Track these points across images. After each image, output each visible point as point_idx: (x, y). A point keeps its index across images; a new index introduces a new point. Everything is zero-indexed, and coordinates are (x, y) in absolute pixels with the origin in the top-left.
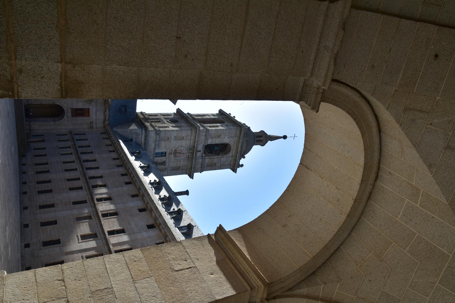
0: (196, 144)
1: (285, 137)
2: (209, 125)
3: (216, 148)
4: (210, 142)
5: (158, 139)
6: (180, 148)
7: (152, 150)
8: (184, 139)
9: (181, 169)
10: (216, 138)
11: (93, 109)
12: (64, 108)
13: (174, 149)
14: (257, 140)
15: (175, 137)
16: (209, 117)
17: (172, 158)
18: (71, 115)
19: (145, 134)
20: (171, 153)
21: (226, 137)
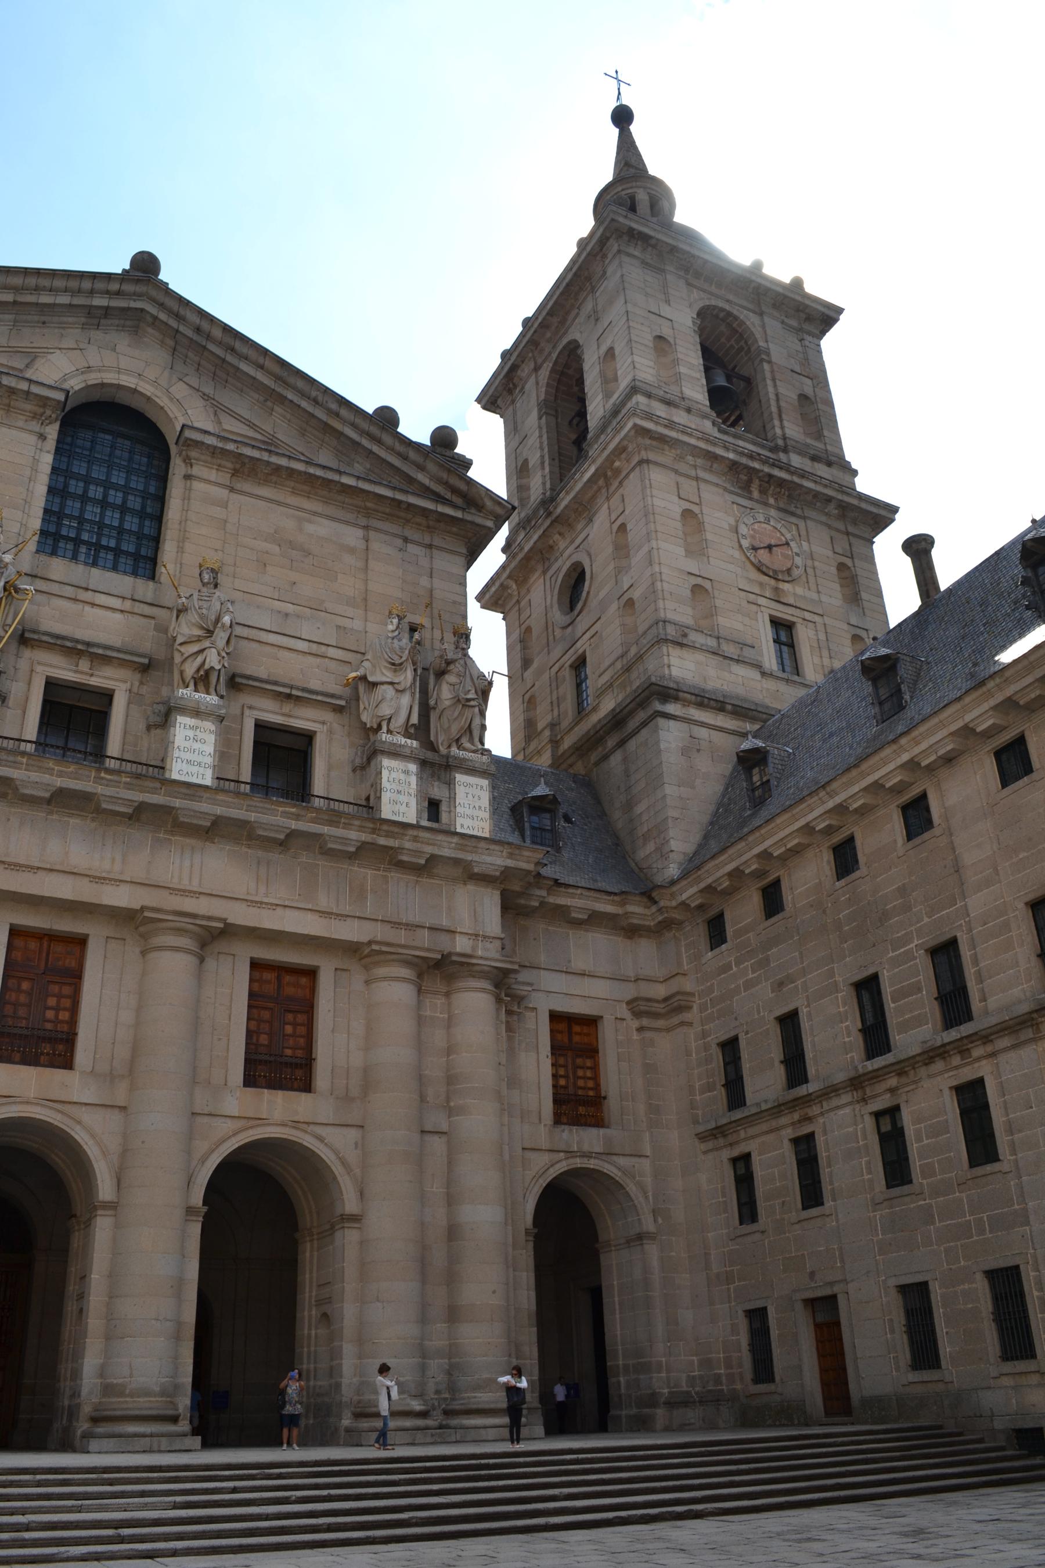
0: (720, 452)
1: (622, 117)
3: (721, 381)
4: (697, 393)
5: (712, 643)
6: (745, 543)
7: (770, 684)
8: (696, 509)
10: (676, 362)
11: (554, 992)
12: (553, 1173)
13: (754, 575)
15: (689, 553)
16: (533, 440)
17: (799, 591)
18: (593, 1132)
19: (687, 703)
20: (776, 589)
21: (666, 311)
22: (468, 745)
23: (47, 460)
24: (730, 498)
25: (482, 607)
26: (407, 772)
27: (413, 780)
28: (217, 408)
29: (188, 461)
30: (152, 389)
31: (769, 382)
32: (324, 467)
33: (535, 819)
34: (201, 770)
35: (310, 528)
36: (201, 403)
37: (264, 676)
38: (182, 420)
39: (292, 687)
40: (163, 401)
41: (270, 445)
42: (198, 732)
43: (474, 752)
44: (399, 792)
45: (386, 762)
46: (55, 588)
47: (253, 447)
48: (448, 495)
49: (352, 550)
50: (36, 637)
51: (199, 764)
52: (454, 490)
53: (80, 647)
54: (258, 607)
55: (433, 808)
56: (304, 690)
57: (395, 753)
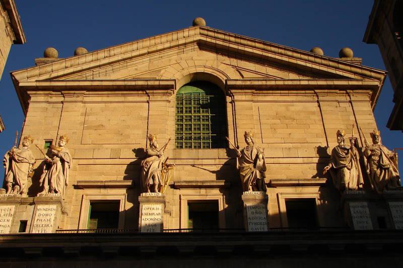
23: (172, 111)
25: (391, 129)
26: (363, 207)
27: (367, 210)
29: (231, 95)
30: (211, 70)
32: (292, 80)
34: (262, 226)
35: (292, 108)
37: (285, 178)
38: (225, 78)
39: (299, 180)
41: (267, 77)
42: (257, 209)
43: (395, 190)
44: (361, 217)
45: (351, 204)
46: (185, 162)
47: (258, 80)
48: (352, 76)
49: (313, 113)
50: (179, 184)
51: (261, 224)
52: (355, 73)
53: (199, 184)
54: (276, 148)
56: (305, 180)
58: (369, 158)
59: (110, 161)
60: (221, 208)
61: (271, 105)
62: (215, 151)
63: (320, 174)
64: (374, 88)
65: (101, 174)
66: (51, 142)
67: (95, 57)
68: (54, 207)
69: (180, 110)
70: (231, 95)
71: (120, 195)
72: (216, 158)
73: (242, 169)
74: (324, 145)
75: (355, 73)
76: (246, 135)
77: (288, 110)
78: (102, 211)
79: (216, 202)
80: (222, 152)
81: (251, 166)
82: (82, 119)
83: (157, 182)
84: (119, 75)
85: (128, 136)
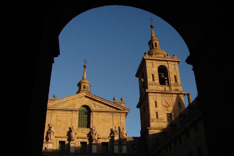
2: (145, 83)
9: (179, 101)
14: (156, 47)
21: (153, 69)
22: (124, 142)
23: (78, 116)
24: (161, 97)
27: (118, 148)
28: (95, 105)
29: (92, 113)
31: (169, 75)
33: (135, 146)
35: (106, 117)
36: (93, 104)
40: (89, 105)
45: (115, 146)
48: (122, 109)
49: (111, 119)
52: (123, 108)
55: (120, 150)
57: (116, 145)
58: (121, 133)
59: (63, 131)
60: (87, 144)
61: (102, 116)
62: (87, 129)
63: (110, 136)
64: (127, 113)
65: (61, 134)
66: (49, 124)
67: (59, 100)
68: (52, 144)
69: (79, 114)
70: (92, 113)
71: (65, 140)
72: (87, 131)
73: (92, 136)
74: (112, 128)
75: (123, 108)
76: (94, 127)
77: (105, 118)
78: (62, 143)
79: (86, 142)
80: (89, 129)
81: (95, 135)
82: (56, 118)
83: (74, 139)
84: (64, 106)
85: (67, 124)
